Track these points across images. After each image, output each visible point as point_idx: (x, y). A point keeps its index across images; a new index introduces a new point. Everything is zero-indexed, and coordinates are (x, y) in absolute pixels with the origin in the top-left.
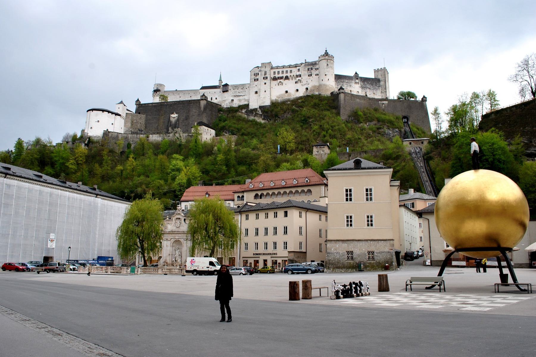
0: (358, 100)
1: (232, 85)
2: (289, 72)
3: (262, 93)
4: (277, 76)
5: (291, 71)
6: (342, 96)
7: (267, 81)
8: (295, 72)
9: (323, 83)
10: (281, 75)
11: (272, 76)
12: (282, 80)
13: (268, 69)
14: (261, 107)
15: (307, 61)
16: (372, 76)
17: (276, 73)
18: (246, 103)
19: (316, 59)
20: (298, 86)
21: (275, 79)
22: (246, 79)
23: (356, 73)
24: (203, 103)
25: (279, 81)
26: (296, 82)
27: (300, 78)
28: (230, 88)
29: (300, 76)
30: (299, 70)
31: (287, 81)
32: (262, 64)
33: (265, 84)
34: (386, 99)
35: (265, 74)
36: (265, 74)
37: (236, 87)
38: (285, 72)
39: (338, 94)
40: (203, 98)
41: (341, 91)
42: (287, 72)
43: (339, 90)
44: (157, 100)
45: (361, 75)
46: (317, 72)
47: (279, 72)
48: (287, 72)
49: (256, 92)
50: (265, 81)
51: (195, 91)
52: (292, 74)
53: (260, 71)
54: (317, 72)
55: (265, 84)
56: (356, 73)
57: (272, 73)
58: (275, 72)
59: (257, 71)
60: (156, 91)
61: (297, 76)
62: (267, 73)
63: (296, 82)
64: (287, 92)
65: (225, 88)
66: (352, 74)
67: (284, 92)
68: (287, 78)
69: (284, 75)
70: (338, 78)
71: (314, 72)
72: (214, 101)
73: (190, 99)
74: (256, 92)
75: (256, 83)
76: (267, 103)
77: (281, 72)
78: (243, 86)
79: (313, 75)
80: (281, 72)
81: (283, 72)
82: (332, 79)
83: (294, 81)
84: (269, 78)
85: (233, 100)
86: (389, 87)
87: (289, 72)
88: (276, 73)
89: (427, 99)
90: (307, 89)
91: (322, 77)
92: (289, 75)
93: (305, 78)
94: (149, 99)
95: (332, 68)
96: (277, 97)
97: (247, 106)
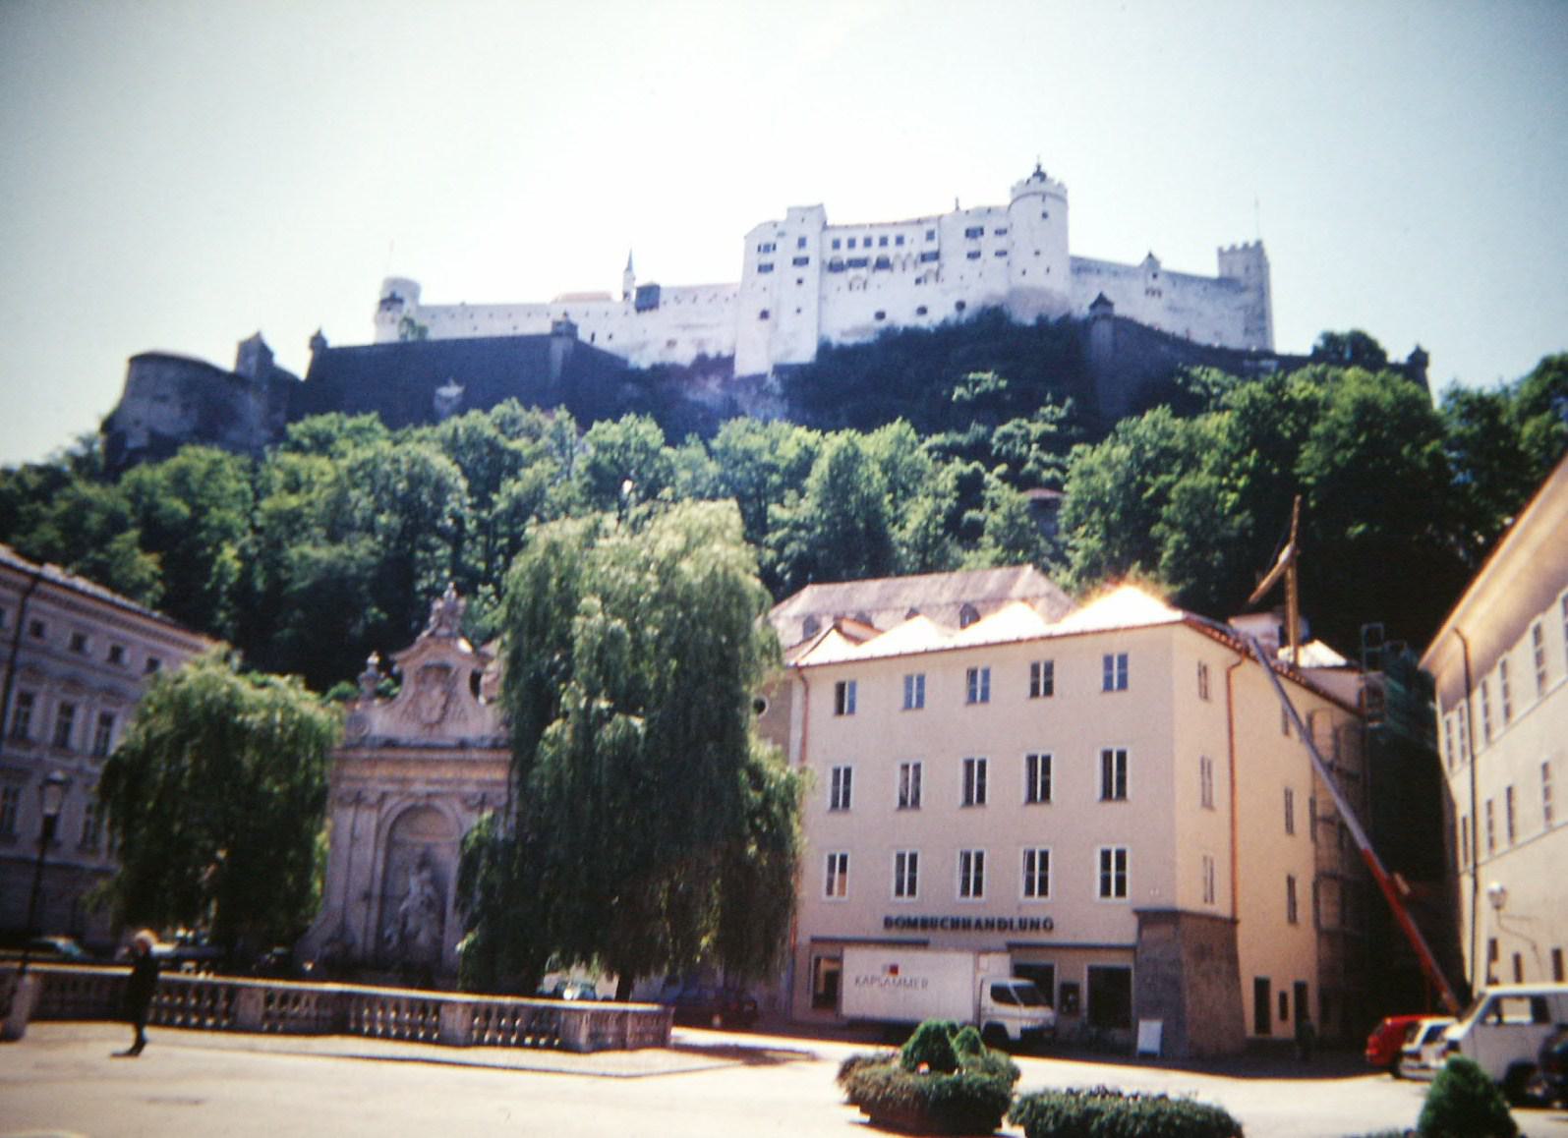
0: (1164, 348)
1: (671, 289)
2: (892, 241)
3: (786, 321)
4: (845, 254)
5: (900, 241)
6: (1103, 330)
7: (810, 273)
8: (916, 244)
9: (1026, 282)
10: (859, 252)
11: (830, 255)
12: (863, 272)
13: (811, 231)
14: (780, 370)
15: (963, 207)
16: (1211, 269)
17: (844, 244)
18: (726, 353)
19: (1003, 199)
20: (928, 295)
21: (835, 267)
22: (728, 266)
23: (1150, 256)
24: (559, 347)
25: (852, 273)
26: (918, 281)
27: (934, 265)
28: (663, 297)
29: (936, 256)
30: (930, 236)
31: (883, 275)
32: (790, 210)
33: (800, 282)
34: (1269, 355)
35: (802, 243)
36: (802, 243)
37: (689, 294)
38: (876, 242)
39: (1086, 325)
40: (562, 328)
41: (1099, 310)
42: (884, 242)
43: (1093, 306)
44: (391, 335)
45: (1168, 263)
46: (1001, 243)
47: (852, 243)
48: (884, 242)
49: (764, 315)
50: (800, 272)
51: (530, 311)
52: (904, 250)
53: (781, 234)
54: (1001, 243)
55: (800, 282)
56: (1150, 256)
57: (829, 244)
58: (836, 245)
59: (771, 238)
60: (391, 301)
61: (924, 258)
62: (809, 242)
63: (918, 281)
64: (880, 316)
65: (648, 298)
66: (1135, 258)
67: (872, 316)
68: (883, 264)
69: (874, 253)
70: (1082, 268)
71: (989, 244)
72: (602, 343)
73: (510, 332)
74: (764, 315)
75: (765, 278)
76: (805, 353)
77: (860, 242)
78: (714, 294)
79: (988, 254)
80: (860, 242)
81: (868, 242)
82: (1062, 270)
83: (912, 274)
84: (812, 262)
85: (671, 344)
86: (1270, 316)
87: (892, 241)
88: (844, 244)
89: (1433, 360)
90: (961, 306)
91: (1021, 257)
92: (891, 251)
93: (955, 261)
94: (358, 328)
95: (1063, 229)
96: (844, 334)
97: (725, 364)
